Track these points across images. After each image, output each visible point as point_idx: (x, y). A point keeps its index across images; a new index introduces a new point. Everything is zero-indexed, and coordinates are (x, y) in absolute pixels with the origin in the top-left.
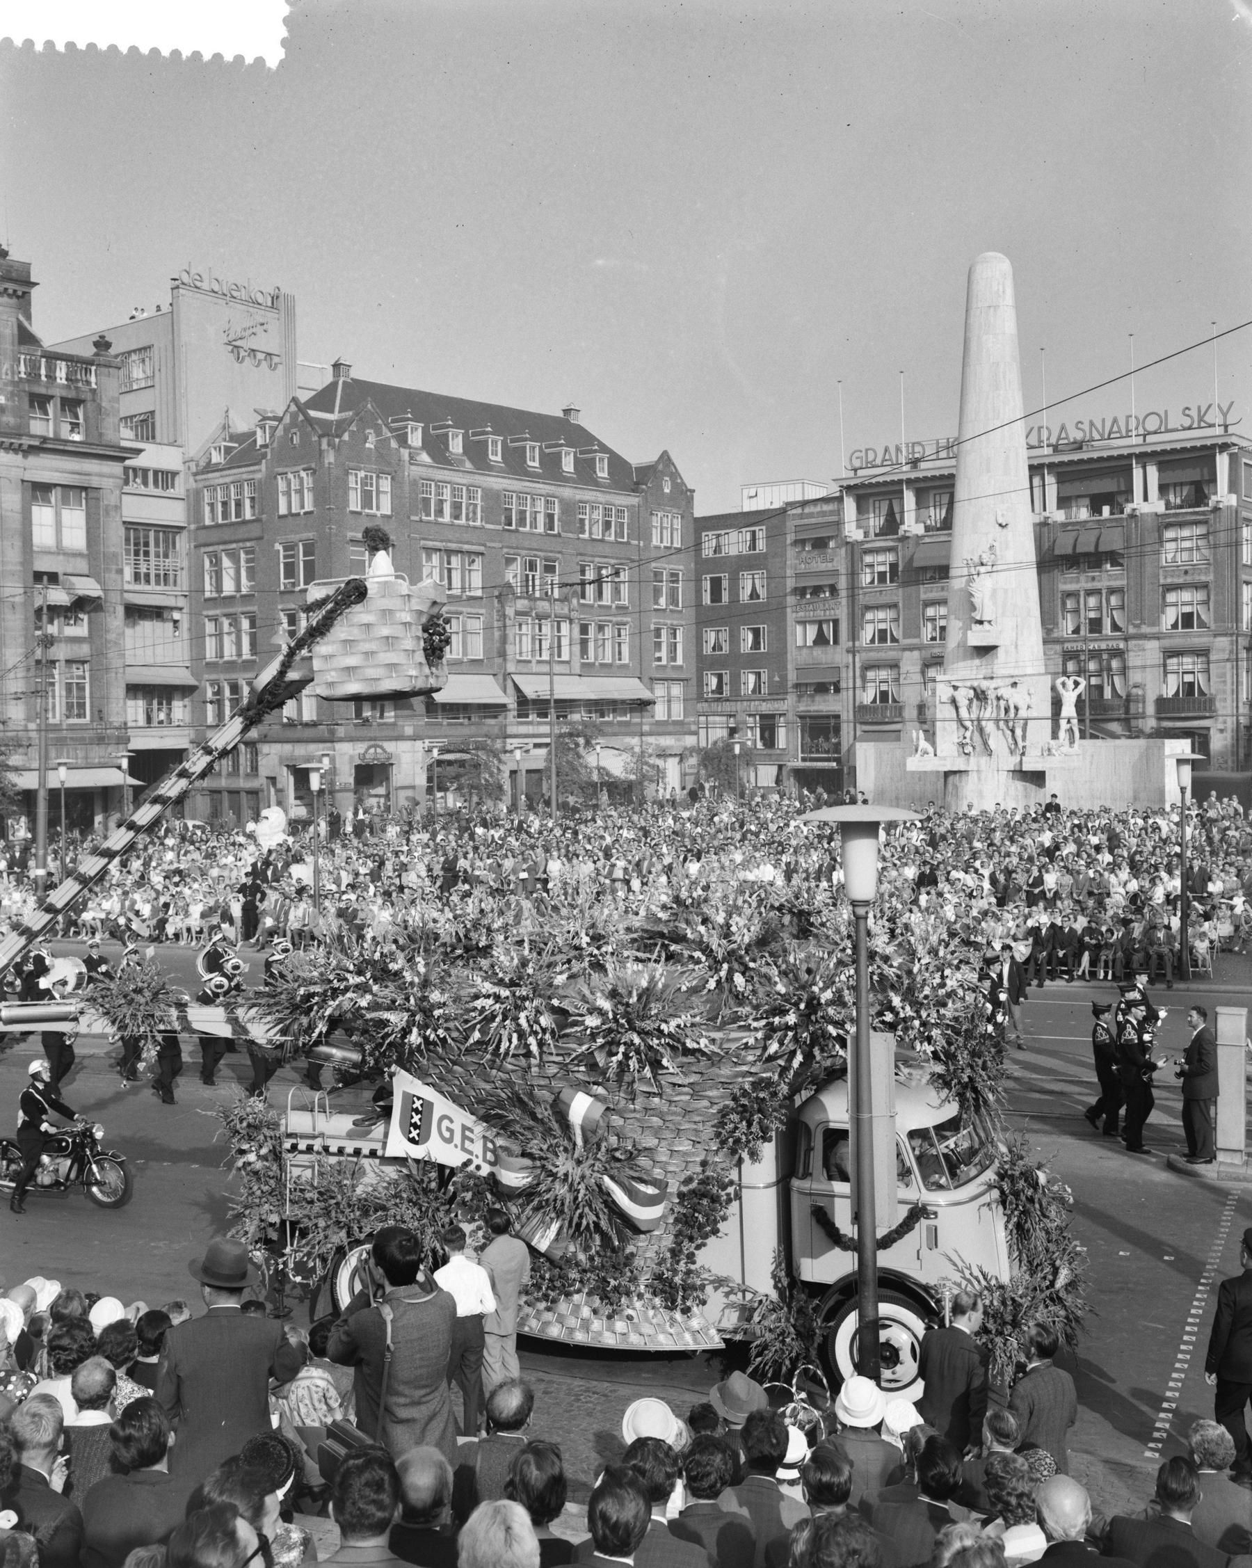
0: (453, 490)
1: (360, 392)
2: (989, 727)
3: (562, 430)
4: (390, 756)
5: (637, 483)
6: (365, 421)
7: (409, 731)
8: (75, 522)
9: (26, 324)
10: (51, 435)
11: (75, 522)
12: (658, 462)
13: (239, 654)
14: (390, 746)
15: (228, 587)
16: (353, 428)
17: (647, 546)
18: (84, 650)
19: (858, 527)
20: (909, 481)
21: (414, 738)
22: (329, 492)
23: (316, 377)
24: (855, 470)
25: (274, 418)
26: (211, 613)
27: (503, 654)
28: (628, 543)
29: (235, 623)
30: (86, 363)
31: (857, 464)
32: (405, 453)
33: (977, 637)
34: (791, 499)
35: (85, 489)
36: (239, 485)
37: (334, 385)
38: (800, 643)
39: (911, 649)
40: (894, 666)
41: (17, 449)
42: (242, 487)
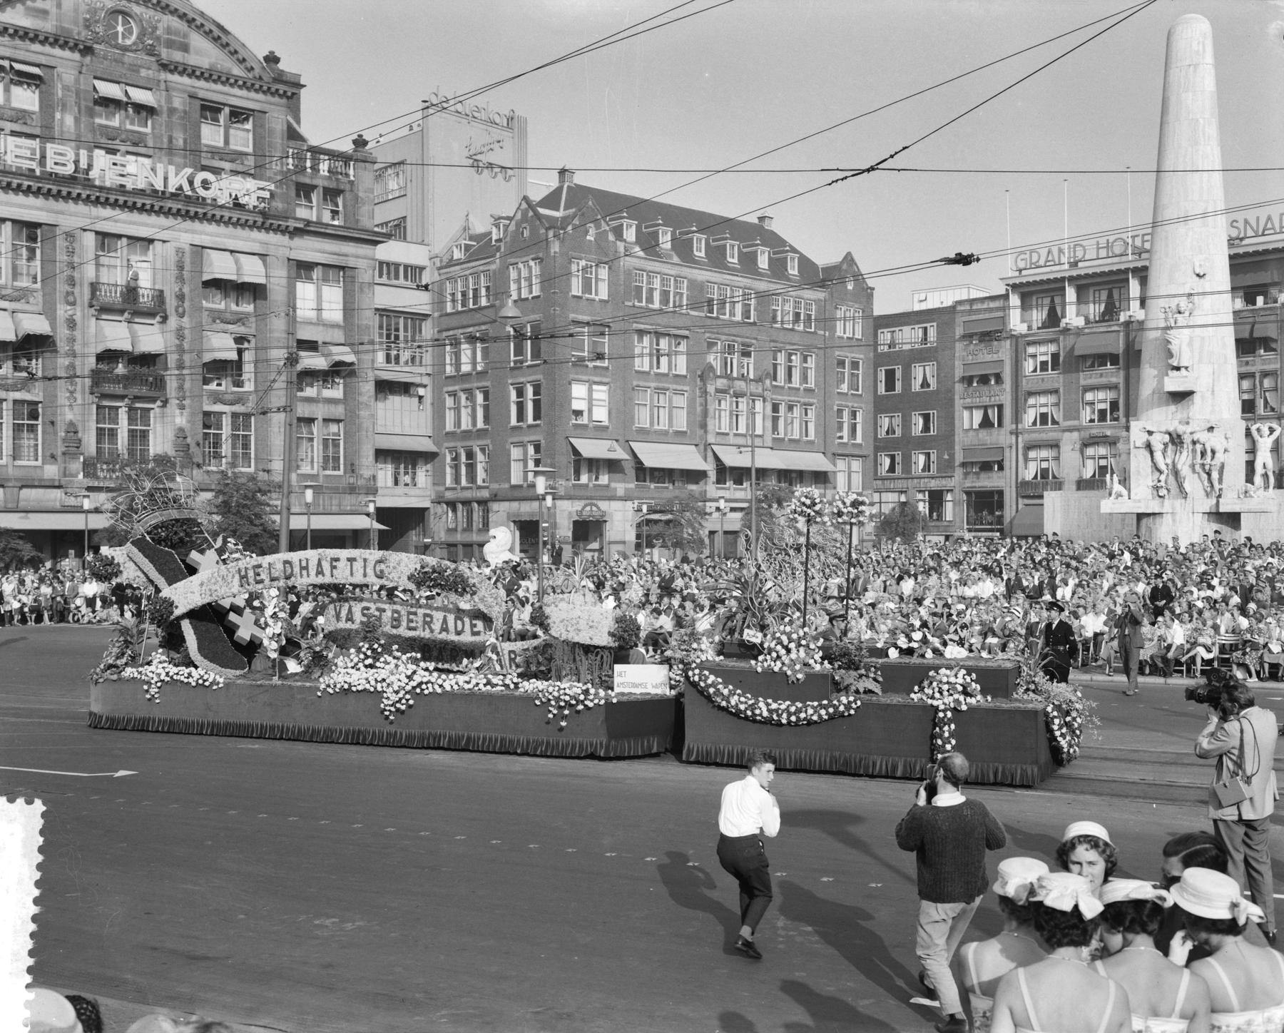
0: (663, 280)
1: (580, 195)
2: (1185, 471)
3: (755, 233)
4: (604, 514)
5: (824, 280)
6: (588, 219)
7: (620, 492)
8: (333, 296)
9: (295, 125)
10: (314, 219)
11: (333, 296)
12: (842, 262)
13: (474, 424)
14: (604, 505)
15: (466, 368)
16: (576, 222)
17: (832, 336)
18: (339, 411)
19: (1023, 321)
20: (1071, 279)
21: (625, 499)
22: (554, 279)
23: (540, 185)
24: (1020, 271)
25: (508, 218)
26: (451, 389)
27: (704, 426)
28: (815, 333)
29: (471, 398)
30: (346, 158)
31: (1022, 265)
32: (621, 246)
33: (1173, 383)
34: (958, 299)
35: (343, 268)
36: (476, 275)
37: (559, 190)
38: (966, 426)
39: (1070, 430)
40: (1055, 445)
41: (285, 231)
42: (479, 277)
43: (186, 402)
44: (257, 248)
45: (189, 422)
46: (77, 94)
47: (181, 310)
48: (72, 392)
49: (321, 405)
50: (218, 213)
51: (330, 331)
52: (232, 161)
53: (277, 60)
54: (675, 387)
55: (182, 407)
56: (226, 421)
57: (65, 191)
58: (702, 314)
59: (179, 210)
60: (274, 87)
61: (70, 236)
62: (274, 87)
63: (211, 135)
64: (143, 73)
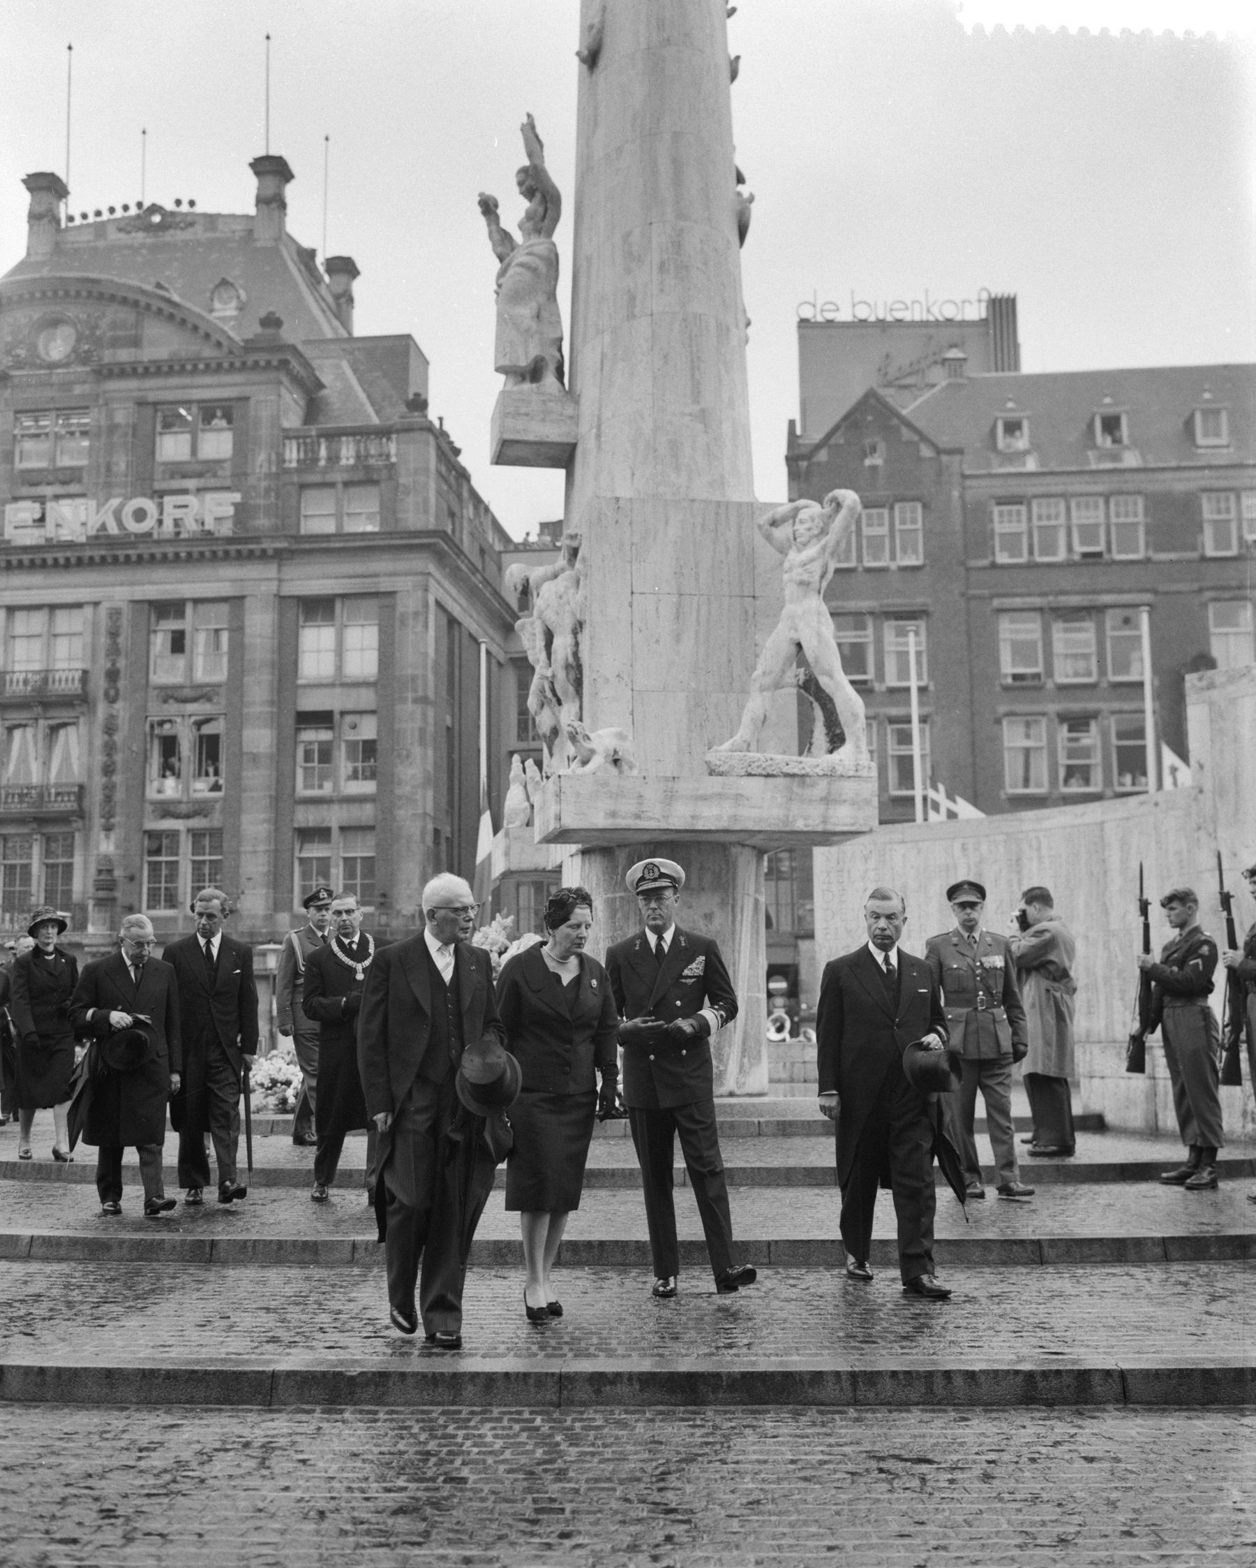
18: (366, 813)
44: (225, 589)
45: (117, 847)
47: (112, 692)
49: (336, 807)
50: (158, 551)
51: (353, 692)
52: (200, 475)
53: (278, 323)
54: (1116, 706)
55: (108, 829)
56: (186, 844)
58: (1194, 555)
59: (103, 558)
60: (250, 359)
62: (250, 359)
63: (172, 447)
64: (78, 390)
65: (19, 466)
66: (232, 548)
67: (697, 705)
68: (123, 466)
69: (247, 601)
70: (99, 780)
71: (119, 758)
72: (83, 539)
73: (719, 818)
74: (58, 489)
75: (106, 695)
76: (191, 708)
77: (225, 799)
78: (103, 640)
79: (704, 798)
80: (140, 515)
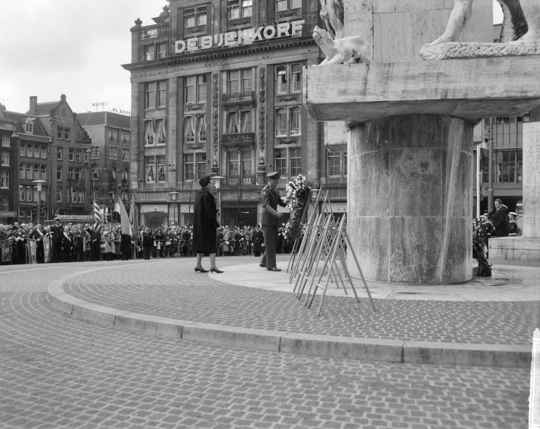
43: (265, 145)
46: (221, 11)
48: (216, 147)
52: (290, 15)
55: (262, 149)
57: (209, 56)
59: (257, 49)
61: (216, 76)
65: (230, 19)
66: (302, 41)
67: (419, 20)
68: (264, 15)
69: (308, 62)
70: (258, 131)
71: (265, 123)
72: (250, 43)
73: (424, 91)
74: (242, 26)
75: (260, 100)
76: (289, 103)
77: (302, 136)
78: (258, 80)
79: (413, 77)
80: (269, 32)
